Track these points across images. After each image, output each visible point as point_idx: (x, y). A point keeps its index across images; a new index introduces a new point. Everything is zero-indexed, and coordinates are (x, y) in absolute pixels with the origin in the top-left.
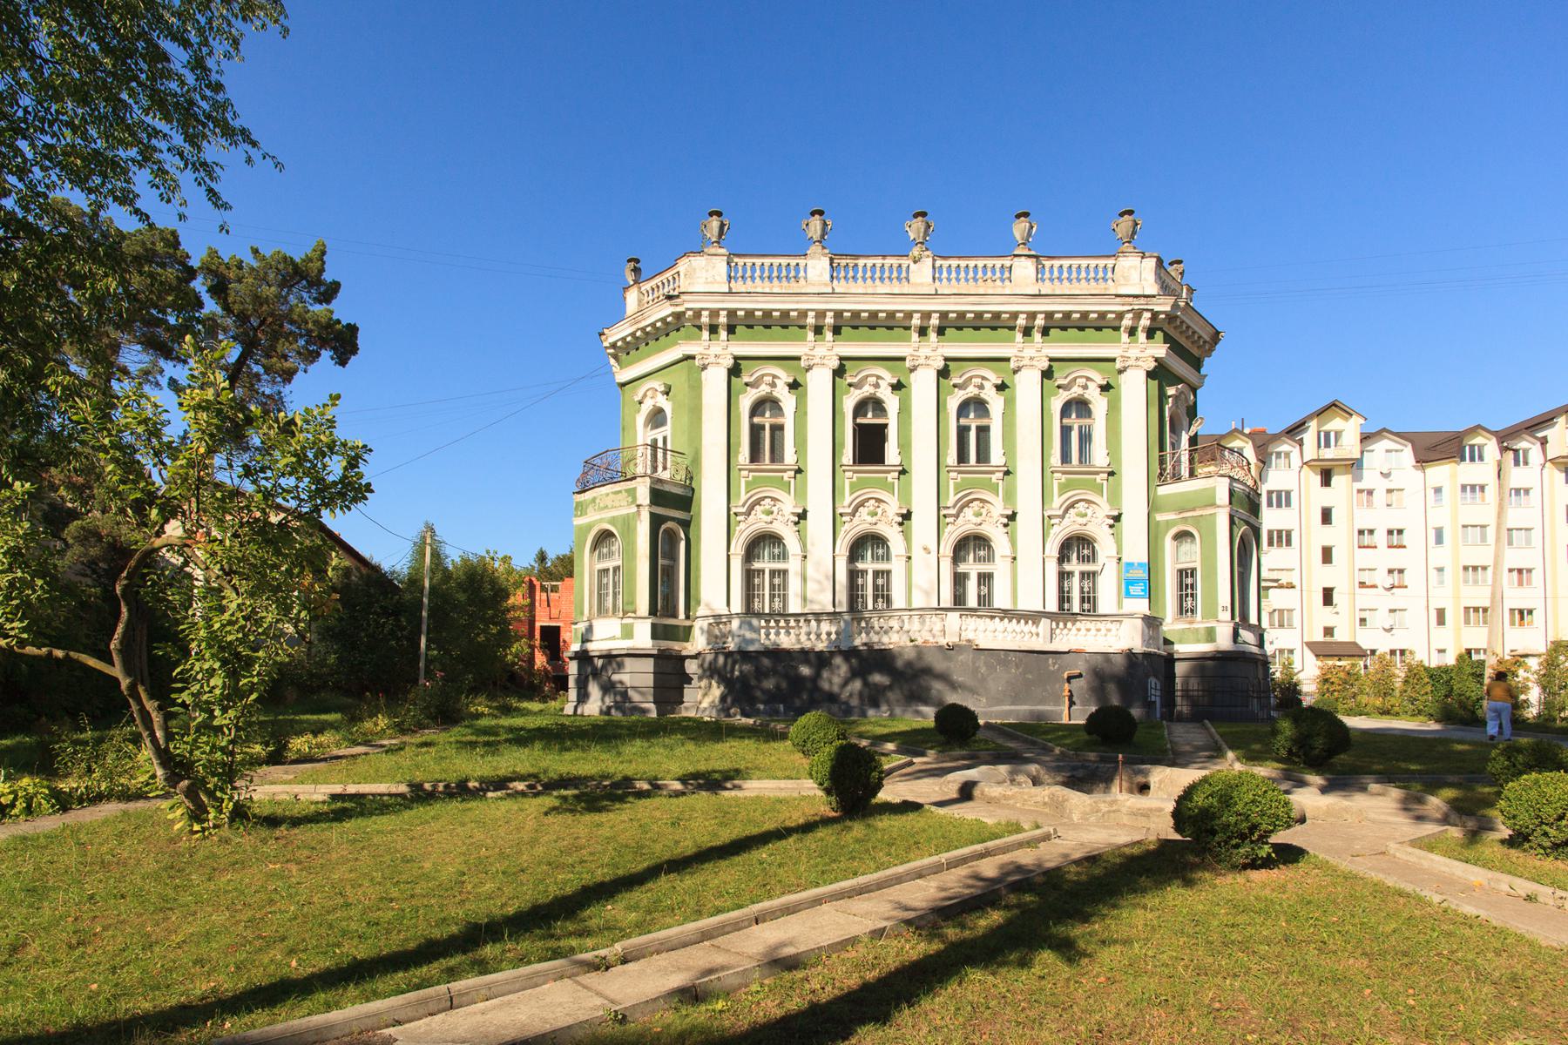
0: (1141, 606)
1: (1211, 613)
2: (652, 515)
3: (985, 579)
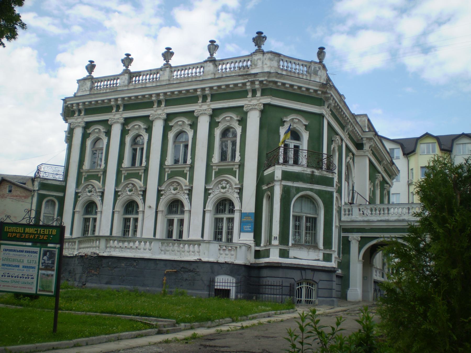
0: (248, 238)
3: (181, 222)
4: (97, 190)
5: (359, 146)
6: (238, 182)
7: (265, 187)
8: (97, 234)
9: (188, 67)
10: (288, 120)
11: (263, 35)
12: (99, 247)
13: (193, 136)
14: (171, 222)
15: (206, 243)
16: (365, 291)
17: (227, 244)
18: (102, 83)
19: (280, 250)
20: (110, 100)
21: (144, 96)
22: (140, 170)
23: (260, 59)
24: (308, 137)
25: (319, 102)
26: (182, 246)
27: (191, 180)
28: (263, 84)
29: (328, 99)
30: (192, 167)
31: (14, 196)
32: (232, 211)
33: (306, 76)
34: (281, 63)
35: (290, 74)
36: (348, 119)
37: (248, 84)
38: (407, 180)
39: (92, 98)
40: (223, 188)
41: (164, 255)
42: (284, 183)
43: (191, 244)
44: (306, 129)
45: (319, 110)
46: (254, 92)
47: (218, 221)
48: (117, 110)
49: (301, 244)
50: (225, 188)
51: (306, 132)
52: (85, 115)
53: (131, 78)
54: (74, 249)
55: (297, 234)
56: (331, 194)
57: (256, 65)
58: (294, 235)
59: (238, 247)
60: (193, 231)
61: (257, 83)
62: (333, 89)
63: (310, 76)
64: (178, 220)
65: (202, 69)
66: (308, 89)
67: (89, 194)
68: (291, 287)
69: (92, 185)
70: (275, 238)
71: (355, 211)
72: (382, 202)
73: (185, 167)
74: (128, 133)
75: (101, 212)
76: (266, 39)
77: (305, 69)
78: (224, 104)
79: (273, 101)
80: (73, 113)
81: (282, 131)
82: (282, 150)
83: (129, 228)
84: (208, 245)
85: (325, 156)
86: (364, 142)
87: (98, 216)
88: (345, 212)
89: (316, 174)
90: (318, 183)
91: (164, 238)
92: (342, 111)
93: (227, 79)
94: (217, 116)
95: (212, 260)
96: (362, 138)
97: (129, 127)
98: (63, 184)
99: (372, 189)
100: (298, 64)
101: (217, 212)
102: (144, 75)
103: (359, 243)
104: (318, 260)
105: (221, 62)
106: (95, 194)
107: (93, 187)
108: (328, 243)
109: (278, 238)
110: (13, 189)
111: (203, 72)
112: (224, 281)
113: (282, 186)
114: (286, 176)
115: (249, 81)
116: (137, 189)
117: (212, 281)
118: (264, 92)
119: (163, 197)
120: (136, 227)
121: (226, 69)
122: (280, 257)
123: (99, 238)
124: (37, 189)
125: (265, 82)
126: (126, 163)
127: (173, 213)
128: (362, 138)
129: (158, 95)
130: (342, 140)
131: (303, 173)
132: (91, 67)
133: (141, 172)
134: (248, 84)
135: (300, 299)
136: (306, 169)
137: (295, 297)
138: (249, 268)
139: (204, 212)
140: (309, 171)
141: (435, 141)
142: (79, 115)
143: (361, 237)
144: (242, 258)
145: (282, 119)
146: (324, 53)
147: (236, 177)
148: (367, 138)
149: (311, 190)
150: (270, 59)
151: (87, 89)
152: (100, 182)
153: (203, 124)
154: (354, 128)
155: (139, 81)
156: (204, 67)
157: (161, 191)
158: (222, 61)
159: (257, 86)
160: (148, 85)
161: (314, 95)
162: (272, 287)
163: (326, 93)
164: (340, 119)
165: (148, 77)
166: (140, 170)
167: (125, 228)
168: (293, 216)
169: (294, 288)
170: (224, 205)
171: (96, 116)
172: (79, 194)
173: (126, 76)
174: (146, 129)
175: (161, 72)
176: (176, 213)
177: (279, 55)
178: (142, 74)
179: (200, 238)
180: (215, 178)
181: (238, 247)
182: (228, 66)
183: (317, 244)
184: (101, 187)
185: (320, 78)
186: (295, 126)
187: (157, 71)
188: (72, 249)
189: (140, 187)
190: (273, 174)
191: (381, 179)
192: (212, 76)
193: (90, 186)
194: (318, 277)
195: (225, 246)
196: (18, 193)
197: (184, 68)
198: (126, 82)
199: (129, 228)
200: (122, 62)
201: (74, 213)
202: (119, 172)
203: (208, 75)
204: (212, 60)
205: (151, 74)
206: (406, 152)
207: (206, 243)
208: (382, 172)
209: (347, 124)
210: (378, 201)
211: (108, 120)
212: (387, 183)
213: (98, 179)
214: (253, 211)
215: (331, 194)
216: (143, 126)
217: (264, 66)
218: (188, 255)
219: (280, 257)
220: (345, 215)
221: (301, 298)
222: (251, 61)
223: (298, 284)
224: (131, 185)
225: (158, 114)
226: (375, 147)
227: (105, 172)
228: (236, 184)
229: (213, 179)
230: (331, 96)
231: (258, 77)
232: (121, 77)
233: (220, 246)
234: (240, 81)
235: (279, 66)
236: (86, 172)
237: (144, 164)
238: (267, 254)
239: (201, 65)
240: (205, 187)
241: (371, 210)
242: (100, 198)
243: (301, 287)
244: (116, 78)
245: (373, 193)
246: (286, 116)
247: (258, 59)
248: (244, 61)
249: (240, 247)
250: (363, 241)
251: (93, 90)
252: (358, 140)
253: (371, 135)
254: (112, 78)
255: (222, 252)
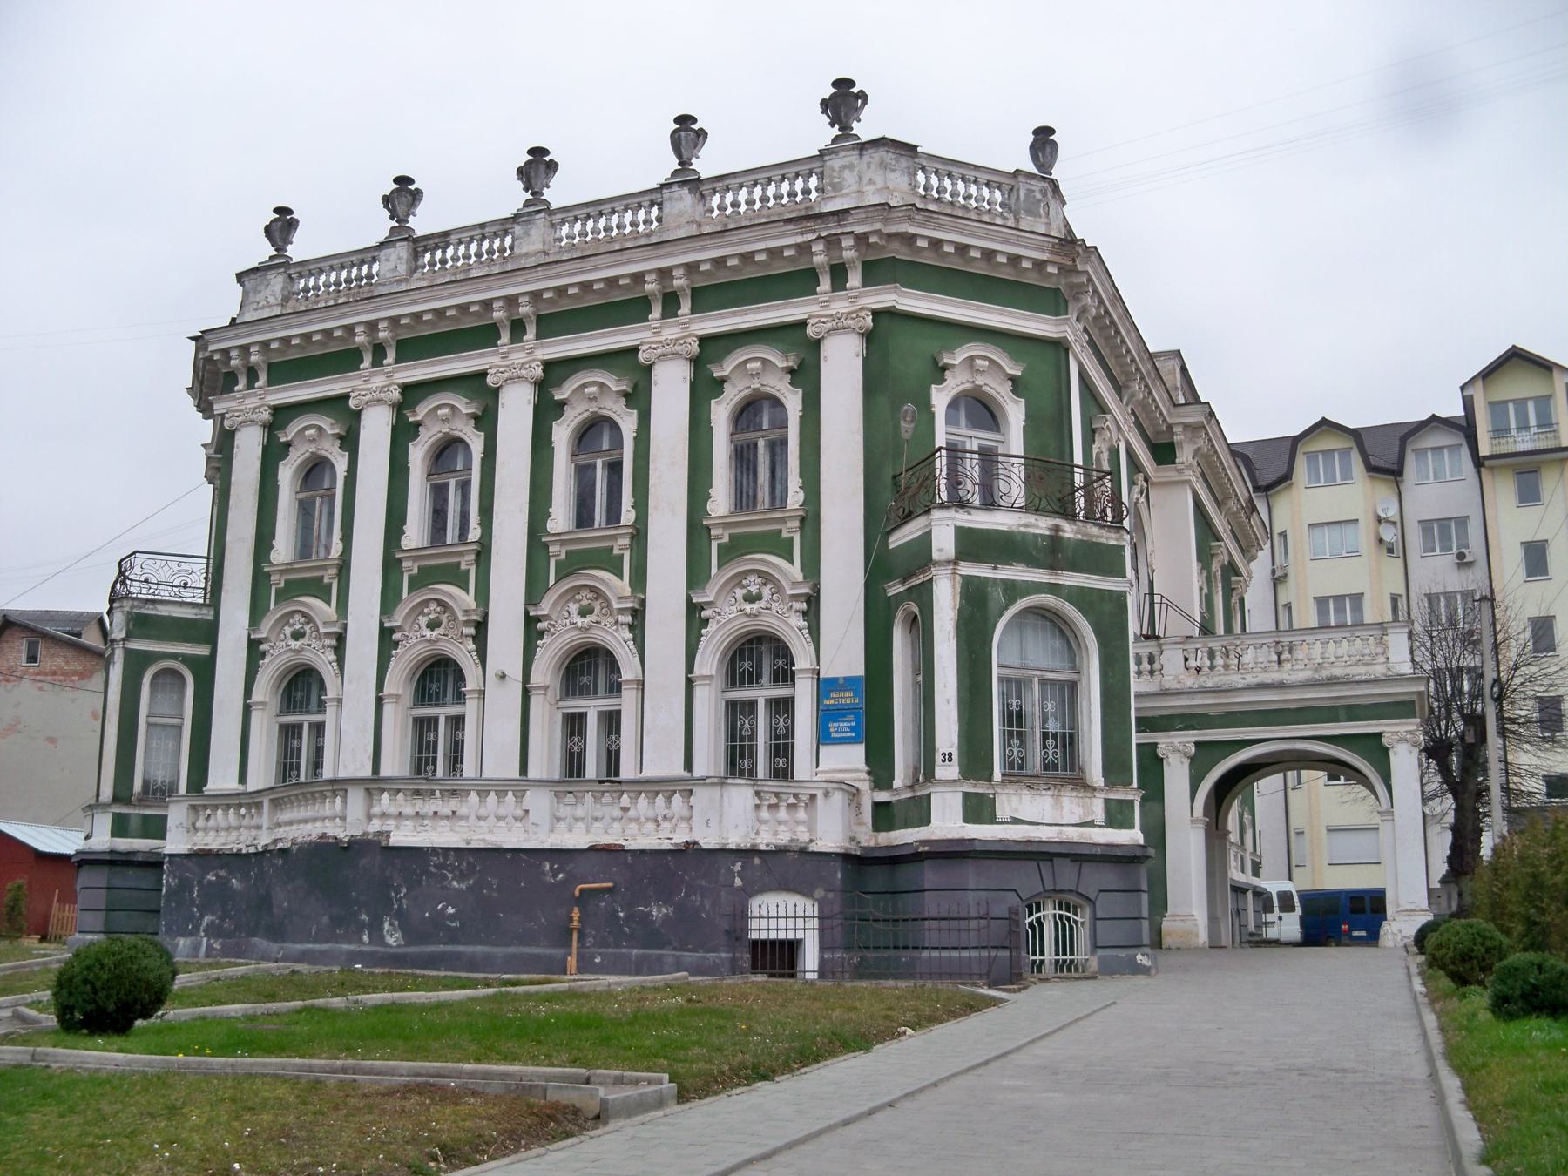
0: (850, 759)
1: (925, 768)
2: (127, 652)
3: (612, 721)
4: (322, 630)
5: (1164, 452)
6: (799, 577)
7: (895, 589)
8: (327, 773)
9: (607, 208)
10: (957, 362)
11: (855, 90)
12: (343, 818)
13: (638, 431)
14: (574, 724)
15: (712, 784)
16: (1213, 919)
17: (774, 786)
18: (323, 278)
19: (966, 795)
20: (350, 330)
21: (462, 308)
22: (461, 553)
23: (851, 167)
24: (1023, 417)
25: (1051, 301)
26: (625, 800)
27: (639, 579)
28: (869, 245)
29: (1077, 291)
30: (639, 536)
31: (46, 674)
32: (786, 675)
33: (1005, 218)
34: (921, 177)
35: (956, 214)
36: (1133, 360)
37: (818, 248)
38: (1269, 567)
39: (292, 327)
40: (750, 599)
41: (567, 835)
42: (967, 569)
43: (658, 793)
44: (1016, 391)
45: (1053, 328)
46: (839, 274)
47: (737, 712)
48: (377, 362)
49: (1030, 772)
50: (759, 597)
51: (1016, 402)
52: (270, 383)
53: (416, 255)
54: (259, 827)
55: (1015, 741)
56: (1119, 599)
57: (837, 187)
58: (1007, 744)
59: (820, 794)
60: (654, 746)
61: (847, 242)
62: (1093, 258)
63: (1017, 220)
64: (600, 714)
65: (655, 211)
66: (1014, 260)
67: (294, 644)
68: (1012, 919)
69: (304, 614)
70: (948, 757)
71: (1171, 661)
72: (1229, 629)
73: (614, 537)
74: (416, 435)
75: (340, 701)
76: (865, 102)
77: (998, 195)
78: (738, 319)
79: (901, 300)
80: (230, 380)
81: (940, 399)
82: (941, 463)
83: (436, 756)
84: (716, 791)
85: (1079, 479)
86: (1177, 438)
87: (329, 717)
88: (1139, 662)
89: (1067, 535)
90: (1074, 567)
91: (557, 776)
92: (1118, 332)
93: (745, 235)
94: (719, 359)
95: (735, 840)
96: (1170, 427)
97: (422, 411)
98: (208, 614)
99: (1205, 590)
100: (975, 182)
101: (733, 683)
102: (460, 243)
103: (1191, 765)
104: (1091, 824)
105: (718, 185)
106: (314, 643)
107: (309, 619)
108: (1115, 768)
109: (955, 757)
110: (41, 651)
111: (659, 220)
112: (781, 914)
113: (958, 579)
114: (972, 545)
115: (819, 237)
116: (455, 619)
117: (742, 916)
118: (875, 272)
119: (546, 640)
120: (457, 748)
121: (735, 204)
122: (966, 820)
123: (340, 786)
124: (123, 635)
125: (873, 239)
126: (415, 533)
127: (581, 693)
128: (1170, 427)
129: (511, 301)
130: (1119, 428)
131: (1024, 534)
132: (282, 225)
133: (467, 562)
134: (818, 248)
135: (1038, 958)
136: (1031, 519)
137: (1024, 954)
138: (856, 862)
139: (690, 684)
140: (1041, 525)
141: (1349, 443)
142: (250, 386)
143: (1197, 744)
144: (832, 830)
145: (935, 362)
146: (1054, 145)
147: (792, 562)
148: (1186, 426)
149: (1054, 589)
150: (883, 165)
151: (271, 300)
152: (329, 603)
153: (671, 390)
154: (1150, 393)
155: (444, 262)
156: (660, 206)
157: (538, 619)
158: (723, 182)
159: (848, 254)
160: (474, 274)
161: (1033, 279)
162: (954, 924)
163: (1074, 271)
164: (1111, 362)
165: (474, 247)
166: (461, 553)
167: (420, 752)
168: (1001, 680)
169: (1017, 923)
170: (757, 655)
171: (308, 386)
172: (263, 647)
173: (403, 250)
174: (476, 418)
175: (518, 229)
176: (592, 691)
177: (911, 149)
178: (454, 237)
179: (682, 773)
180: (719, 567)
181: (820, 794)
182: (743, 195)
183: (1081, 769)
184: (335, 617)
185: (1048, 224)
186: (980, 381)
187: (504, 226)
188: (249, 828)
189: (466, 612)
190: (926, 539)
191: (1227, 559)
192: (694, 231)
193: (297, 617)
194: (1096, 879)
195: (777, 794)
196: (59, 662)
197: (593, 211)
198: (403, 269)
199: (435, 751)
200: (386, 207)
201: (247, 710)
202: (391, 565)
203: (679, 227)
204: (686, 178)
205: (484, 237)
206: (1262, 483)
207: (712, 784)
208: (1224, 536)
209: (1129, 377)
210: (1220, 629)
211: (346, 397)
212: (1238, 573)
213: (322, 592)
214: (859, 670)
215: (1119, 599)
216: (465, 406)
217: (865, 185)
218: (645, 829)
219: (966, 820)
220: (1139, 673)
221: (1042, 953)
222: (821, 177)
223: (1030, 907)
224: (433, 606)
225: (513, 366)
226: (1206, 457)
227: (344, 567)
228: (795, 584)
229: (714, 570)
230: (1090, 280)
231: (851, 224)
232: (383, 254)
233: (758, 793)
234: (789, 239)
235: (916, 186)
236: (282, 572)
237: (474, 533)
238: (919, 812)
239: (654, 197)
240: (689, 599)
241: (1211, 654)
242: (332, 657)
243: (1038, 920)
244: (368, 256)
245: (1208, 601)
246: (951, 350)
247: (844, 167)
248: (797, 175)
249: (827, 794)
250: (1205, 755)
251: (292, 302)
252: (1158, 433)
253: (1192, 416)
254: (353, 258)
255: (765, 814)
